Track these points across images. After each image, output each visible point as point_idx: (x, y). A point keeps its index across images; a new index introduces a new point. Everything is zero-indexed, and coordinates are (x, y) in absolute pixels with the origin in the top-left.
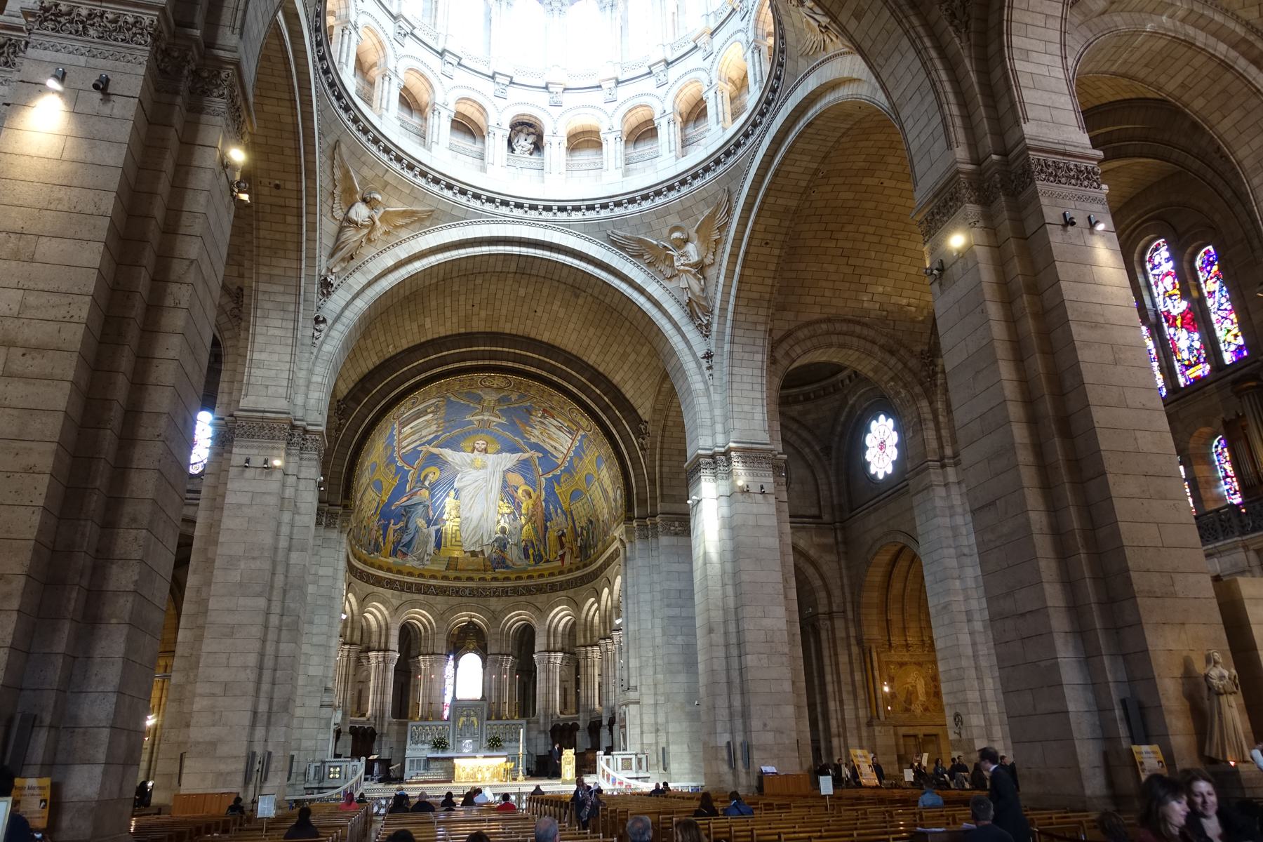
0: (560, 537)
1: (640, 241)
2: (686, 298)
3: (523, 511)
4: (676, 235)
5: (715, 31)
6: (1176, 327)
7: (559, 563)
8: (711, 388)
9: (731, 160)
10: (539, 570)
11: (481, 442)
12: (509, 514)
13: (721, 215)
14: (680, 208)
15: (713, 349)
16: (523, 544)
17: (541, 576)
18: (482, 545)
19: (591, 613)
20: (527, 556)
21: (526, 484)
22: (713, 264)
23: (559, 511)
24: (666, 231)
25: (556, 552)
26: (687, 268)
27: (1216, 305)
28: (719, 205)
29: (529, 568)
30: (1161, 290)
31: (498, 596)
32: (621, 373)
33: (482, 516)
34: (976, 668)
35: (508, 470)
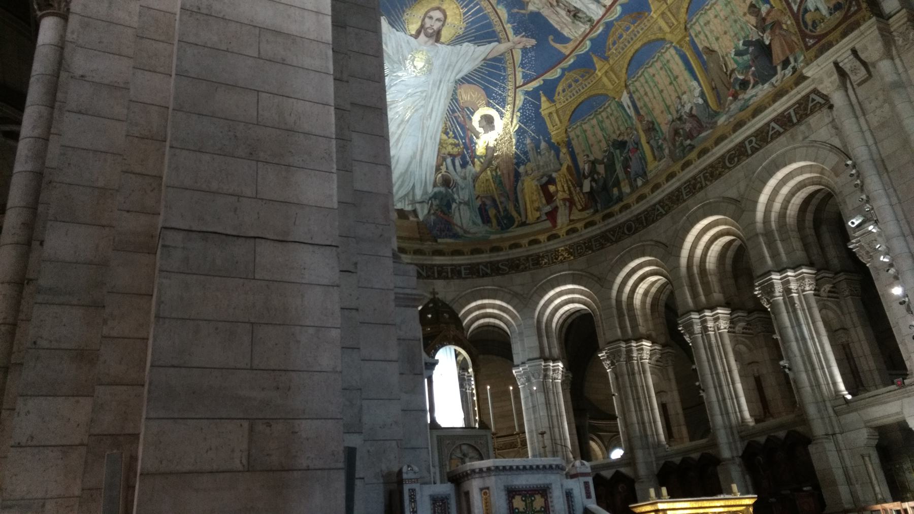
0: (544, 188)
3: (480, 149)
7: (548, 224)
10: (509, 239)
11: (437, 14)
12: (453, 157)
16: (478, 203)
17: (516, 246)
18: (413, 202)
19: (628, 289)
20: (486, 220)
21: (489, 105)
23: (543, 145)
25: (538, 209)
29: (493, 237)
31: (446, 278)
33: (413, 157)
35: (466, 80)
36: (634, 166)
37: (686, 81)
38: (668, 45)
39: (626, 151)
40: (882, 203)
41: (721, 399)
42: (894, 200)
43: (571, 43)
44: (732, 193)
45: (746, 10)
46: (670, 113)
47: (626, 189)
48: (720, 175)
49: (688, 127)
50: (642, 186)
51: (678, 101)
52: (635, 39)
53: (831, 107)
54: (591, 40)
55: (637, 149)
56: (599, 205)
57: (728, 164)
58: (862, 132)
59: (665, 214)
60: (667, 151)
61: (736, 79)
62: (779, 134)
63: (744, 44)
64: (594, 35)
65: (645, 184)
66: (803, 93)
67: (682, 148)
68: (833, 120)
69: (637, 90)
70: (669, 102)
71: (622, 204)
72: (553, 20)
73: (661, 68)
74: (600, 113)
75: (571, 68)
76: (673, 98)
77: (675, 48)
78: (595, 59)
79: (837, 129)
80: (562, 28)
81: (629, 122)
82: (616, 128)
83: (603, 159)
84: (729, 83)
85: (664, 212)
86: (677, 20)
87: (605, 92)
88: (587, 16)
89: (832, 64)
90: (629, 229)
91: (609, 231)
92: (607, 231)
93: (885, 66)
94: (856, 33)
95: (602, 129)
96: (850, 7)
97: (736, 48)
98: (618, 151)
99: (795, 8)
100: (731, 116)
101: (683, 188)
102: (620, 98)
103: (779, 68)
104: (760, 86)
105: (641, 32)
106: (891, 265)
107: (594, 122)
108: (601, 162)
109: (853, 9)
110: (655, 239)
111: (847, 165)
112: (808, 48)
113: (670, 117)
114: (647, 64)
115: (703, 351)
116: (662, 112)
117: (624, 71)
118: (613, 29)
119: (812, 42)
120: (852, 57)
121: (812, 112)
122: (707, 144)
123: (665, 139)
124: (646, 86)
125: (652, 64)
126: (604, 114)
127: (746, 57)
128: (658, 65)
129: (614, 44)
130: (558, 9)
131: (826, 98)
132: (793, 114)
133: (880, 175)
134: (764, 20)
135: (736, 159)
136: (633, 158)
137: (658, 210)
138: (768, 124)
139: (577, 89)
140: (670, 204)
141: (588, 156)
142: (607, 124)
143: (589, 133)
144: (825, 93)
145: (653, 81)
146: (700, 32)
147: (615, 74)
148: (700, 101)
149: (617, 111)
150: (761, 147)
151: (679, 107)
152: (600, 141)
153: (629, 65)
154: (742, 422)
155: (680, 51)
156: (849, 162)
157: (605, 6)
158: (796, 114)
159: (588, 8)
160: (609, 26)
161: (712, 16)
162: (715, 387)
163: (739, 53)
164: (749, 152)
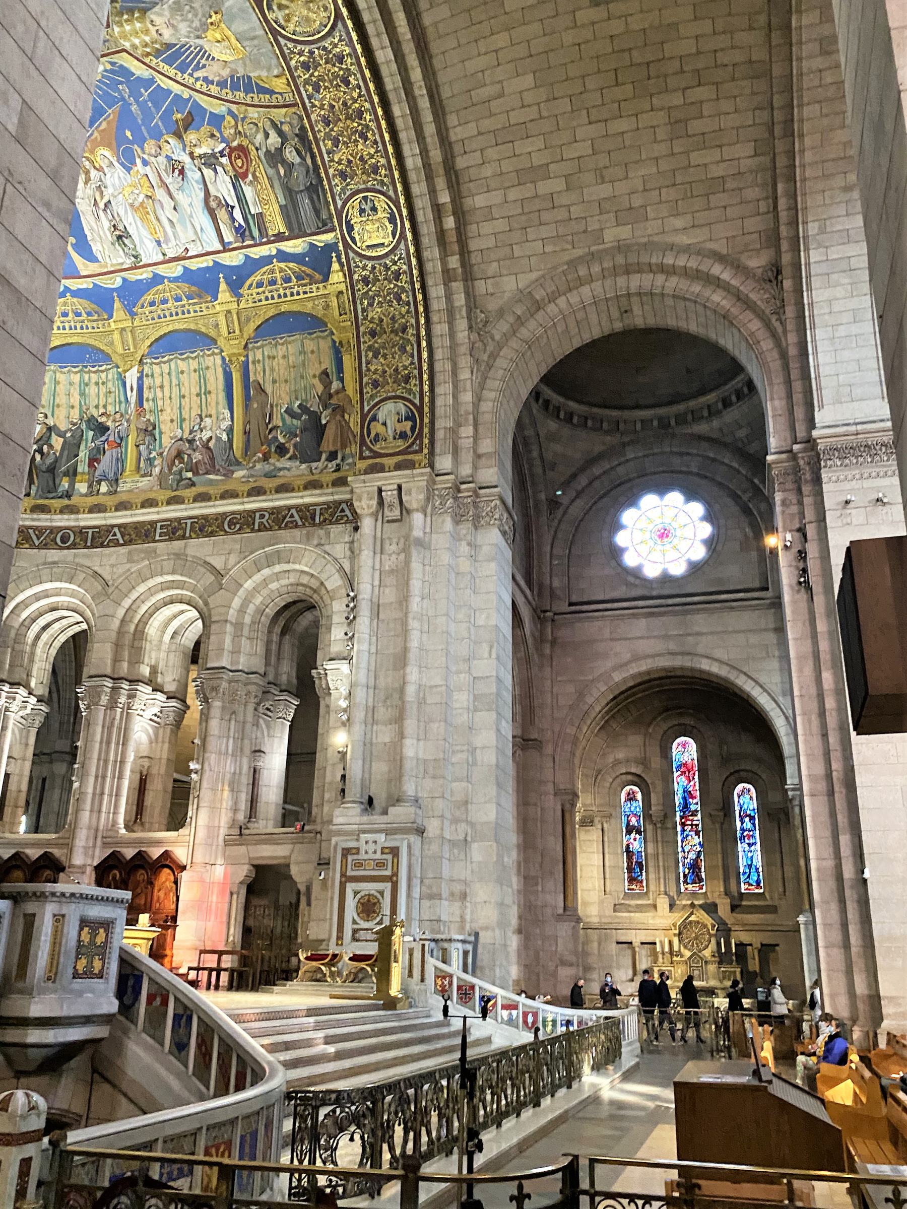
32: (496, 197)
36: (106, 464)
37: (217, 403)
38: (216, 351)
39: (104, 438)
40: (361, 648)
41: (98, 791)
42: (373, 650)
43: (96, 264)
44: (218, 562)
45: (317, 374)
46: (182, 429)
47: (82, 487)
48: (212, 534)
49: (197, 457)
50: (104, 494)
51: (198, 420)
52: (180, 316)
53: (356, 529)
54: (124, 280)
55: (119, 445)
56: (34, 488)
57: (226, 527)
58: (373, 568)
59: (122, 545)
60: (157, 470)
61: (276, 438)
62: (297, 526)
63: (300, 406)
64: (133, 276)
65: (109, 493)
66: (336, 497)
67: (178, 477)
68: (352, 542)
69: (152, 376)
70: (186, 415)
71: (66, 502)
72: (88, 222)
73: (195, 371)
74: (89, 372)
75: (77, 293)
76: (193, 414)
77: (223, 359)
78: (117, 305)
79: (352, 552)
80: (93, 240)
81: (123, 405)
82: (101, 404)
83: (66, 432)
84: (266, 437)
85: (121, 542)
86: (241, 331)
87: (110, 351)
88: (135, 249)
89: (376, 489)
90: (64, 539)
91: (35, 528)
92: (30, 527)
93: (418, 518)
94: (408, 472)
95: (82, 394)
96: (413, 444)
97: (291, 403)
98: (91, 433)
99: (366, 408)
100: (252, 476)
101: (159, 525)
102: (125, 371)
103: (324, 456)
104: (298, 463)
105: (192, 314)
106: (345, 710)
107: (76, 378)
108: (61, 434)
109: (415, 447)
110: (96, 569)
111: (348, 595)
112: (362, 458)
113: (179, 433)
114: (182, 354)
115: (99, 729)
116: (172, 421)
117: (148, 343)
118: (160, 287)
119: (367, 453)
120: (395, 492)
121: (337, 522)
122: (212, 491)
123: (161, 454)
124: (166, 377)
125: (187, 358)
126: (94, 377)
127: (295, 422)
128: (194, 364)
129: (152, 304)
130: (101, 214)
131: (356, 517)
132: (318, 513)
133: (372, 620)
134: (331, 396)
135: (238, 526)
136: (107, 453)
137: (115, 535)
138: (289, 508)
139: (72, 324)
140: (133, 536)
141: (46, 416)
142: (92, 390)
143: (61, 389)
144: (358, 511)
145: (178, 379)
146: (259, 361)
147: (134, 339)
148: (224, 437)
149: (114, 384)
150: (271, 529)
151: (196, 428)
152: (73, 407)
153: (157, 340)
154: (113, 826)
155: (227, 365)
156: (352, 594)
157: (164, 255)
158: (321, 514)
159: (142, 241)
160: (157, 279)
161: (281, 354)
162: (97, 777)
163: (289, 411)
164: (256, 527)
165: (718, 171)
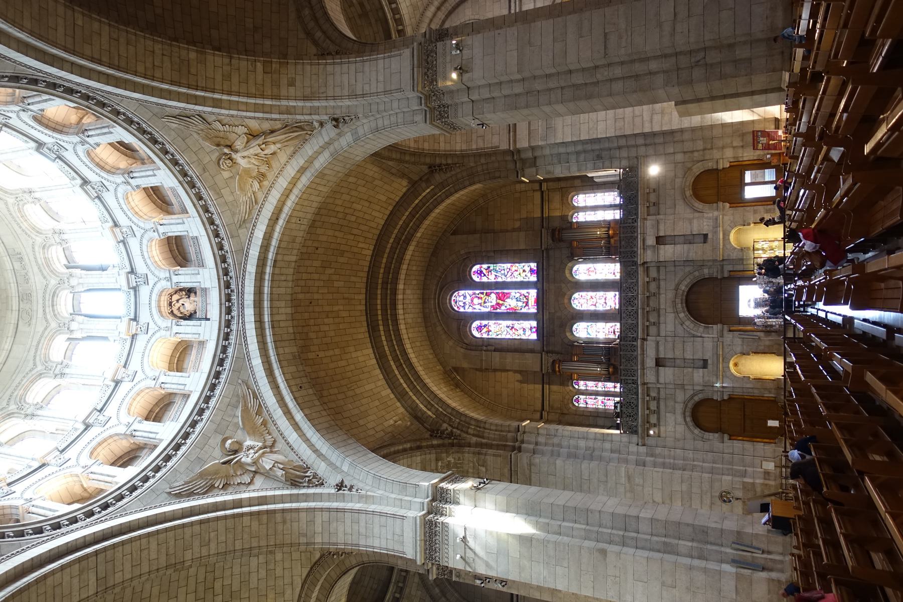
1: (202, 475)
2: (280, 473)
4: (229, 441)
5: (126, 364)
6: (502, 305)
8: (369, 493)
9: (227, 365)
13: (251, 402)
14: (214, 426)
15: (338, 480)
22: (275, 441)
24: (217, 452)
26: (261, 451)
27: (503, 277)
28: (244, 397)
30: (478, 307)
34: (684, 470)
165: (263, 573)
